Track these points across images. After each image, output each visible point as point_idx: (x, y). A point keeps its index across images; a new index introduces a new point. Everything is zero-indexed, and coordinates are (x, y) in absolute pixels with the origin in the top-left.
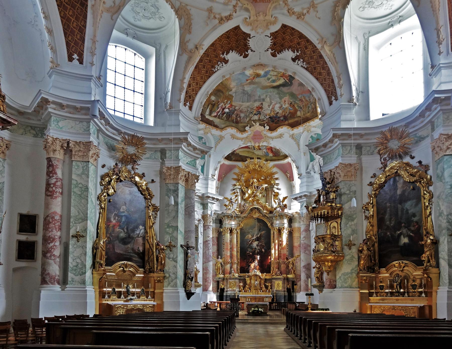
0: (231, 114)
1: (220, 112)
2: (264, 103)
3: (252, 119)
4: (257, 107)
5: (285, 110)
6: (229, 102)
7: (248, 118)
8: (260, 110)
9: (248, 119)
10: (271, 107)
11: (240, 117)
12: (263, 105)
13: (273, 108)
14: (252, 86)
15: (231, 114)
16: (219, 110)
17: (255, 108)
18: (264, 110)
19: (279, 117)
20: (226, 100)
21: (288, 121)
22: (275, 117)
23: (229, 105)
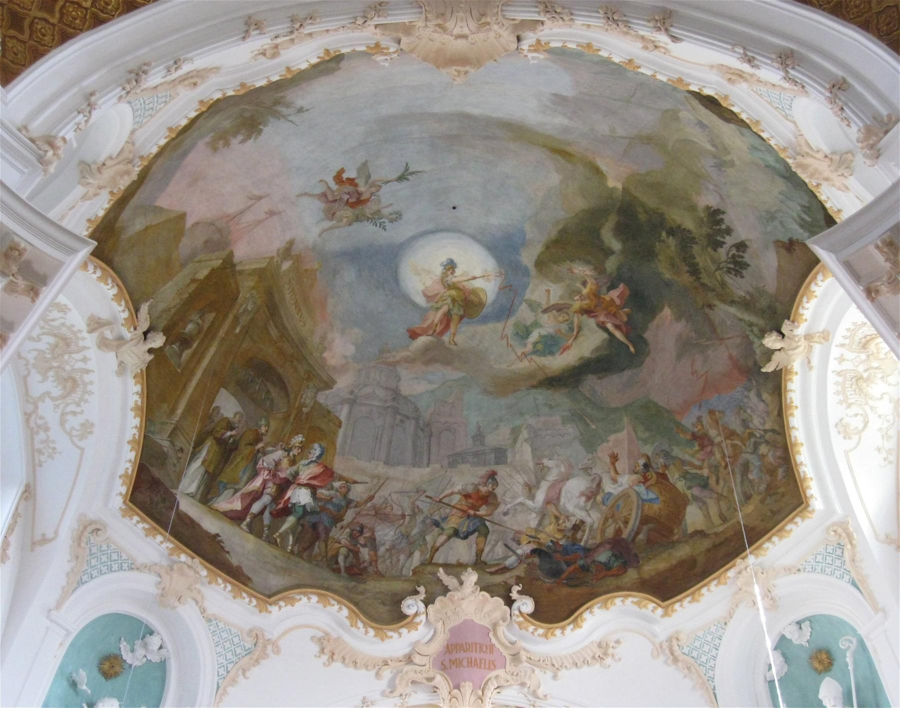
0: (325, 520)
1: (266, 499)
2: (502, 472)
3: (439, 558)
4: (467, 496)
5: (615, 506)
6: (316, 450)
7: (417, 556)
8: (483, 511)
9: (417, 558)
10: (540, 496)
11: (372, 543)
12: (496, 484)
13: (553, 500)
14: (441, 373)
15: (325, 520)
16: (257, 483)
17: (456, 499)
18: (502, 508)
19: (588, 551)
20: (298, 439)
21: (638, 568)
22: (565, 551)
23: (315, 470)
